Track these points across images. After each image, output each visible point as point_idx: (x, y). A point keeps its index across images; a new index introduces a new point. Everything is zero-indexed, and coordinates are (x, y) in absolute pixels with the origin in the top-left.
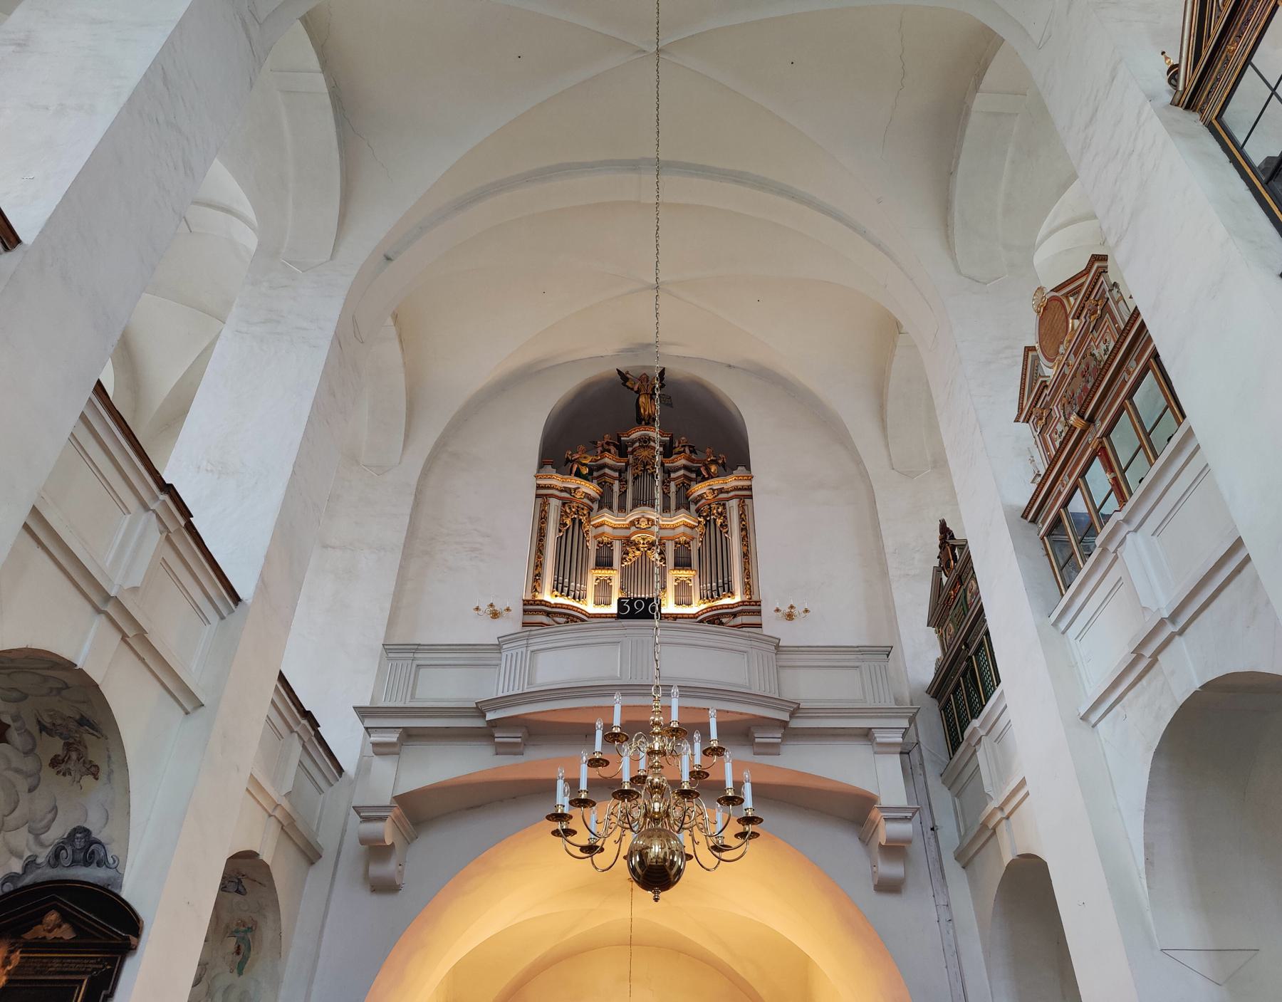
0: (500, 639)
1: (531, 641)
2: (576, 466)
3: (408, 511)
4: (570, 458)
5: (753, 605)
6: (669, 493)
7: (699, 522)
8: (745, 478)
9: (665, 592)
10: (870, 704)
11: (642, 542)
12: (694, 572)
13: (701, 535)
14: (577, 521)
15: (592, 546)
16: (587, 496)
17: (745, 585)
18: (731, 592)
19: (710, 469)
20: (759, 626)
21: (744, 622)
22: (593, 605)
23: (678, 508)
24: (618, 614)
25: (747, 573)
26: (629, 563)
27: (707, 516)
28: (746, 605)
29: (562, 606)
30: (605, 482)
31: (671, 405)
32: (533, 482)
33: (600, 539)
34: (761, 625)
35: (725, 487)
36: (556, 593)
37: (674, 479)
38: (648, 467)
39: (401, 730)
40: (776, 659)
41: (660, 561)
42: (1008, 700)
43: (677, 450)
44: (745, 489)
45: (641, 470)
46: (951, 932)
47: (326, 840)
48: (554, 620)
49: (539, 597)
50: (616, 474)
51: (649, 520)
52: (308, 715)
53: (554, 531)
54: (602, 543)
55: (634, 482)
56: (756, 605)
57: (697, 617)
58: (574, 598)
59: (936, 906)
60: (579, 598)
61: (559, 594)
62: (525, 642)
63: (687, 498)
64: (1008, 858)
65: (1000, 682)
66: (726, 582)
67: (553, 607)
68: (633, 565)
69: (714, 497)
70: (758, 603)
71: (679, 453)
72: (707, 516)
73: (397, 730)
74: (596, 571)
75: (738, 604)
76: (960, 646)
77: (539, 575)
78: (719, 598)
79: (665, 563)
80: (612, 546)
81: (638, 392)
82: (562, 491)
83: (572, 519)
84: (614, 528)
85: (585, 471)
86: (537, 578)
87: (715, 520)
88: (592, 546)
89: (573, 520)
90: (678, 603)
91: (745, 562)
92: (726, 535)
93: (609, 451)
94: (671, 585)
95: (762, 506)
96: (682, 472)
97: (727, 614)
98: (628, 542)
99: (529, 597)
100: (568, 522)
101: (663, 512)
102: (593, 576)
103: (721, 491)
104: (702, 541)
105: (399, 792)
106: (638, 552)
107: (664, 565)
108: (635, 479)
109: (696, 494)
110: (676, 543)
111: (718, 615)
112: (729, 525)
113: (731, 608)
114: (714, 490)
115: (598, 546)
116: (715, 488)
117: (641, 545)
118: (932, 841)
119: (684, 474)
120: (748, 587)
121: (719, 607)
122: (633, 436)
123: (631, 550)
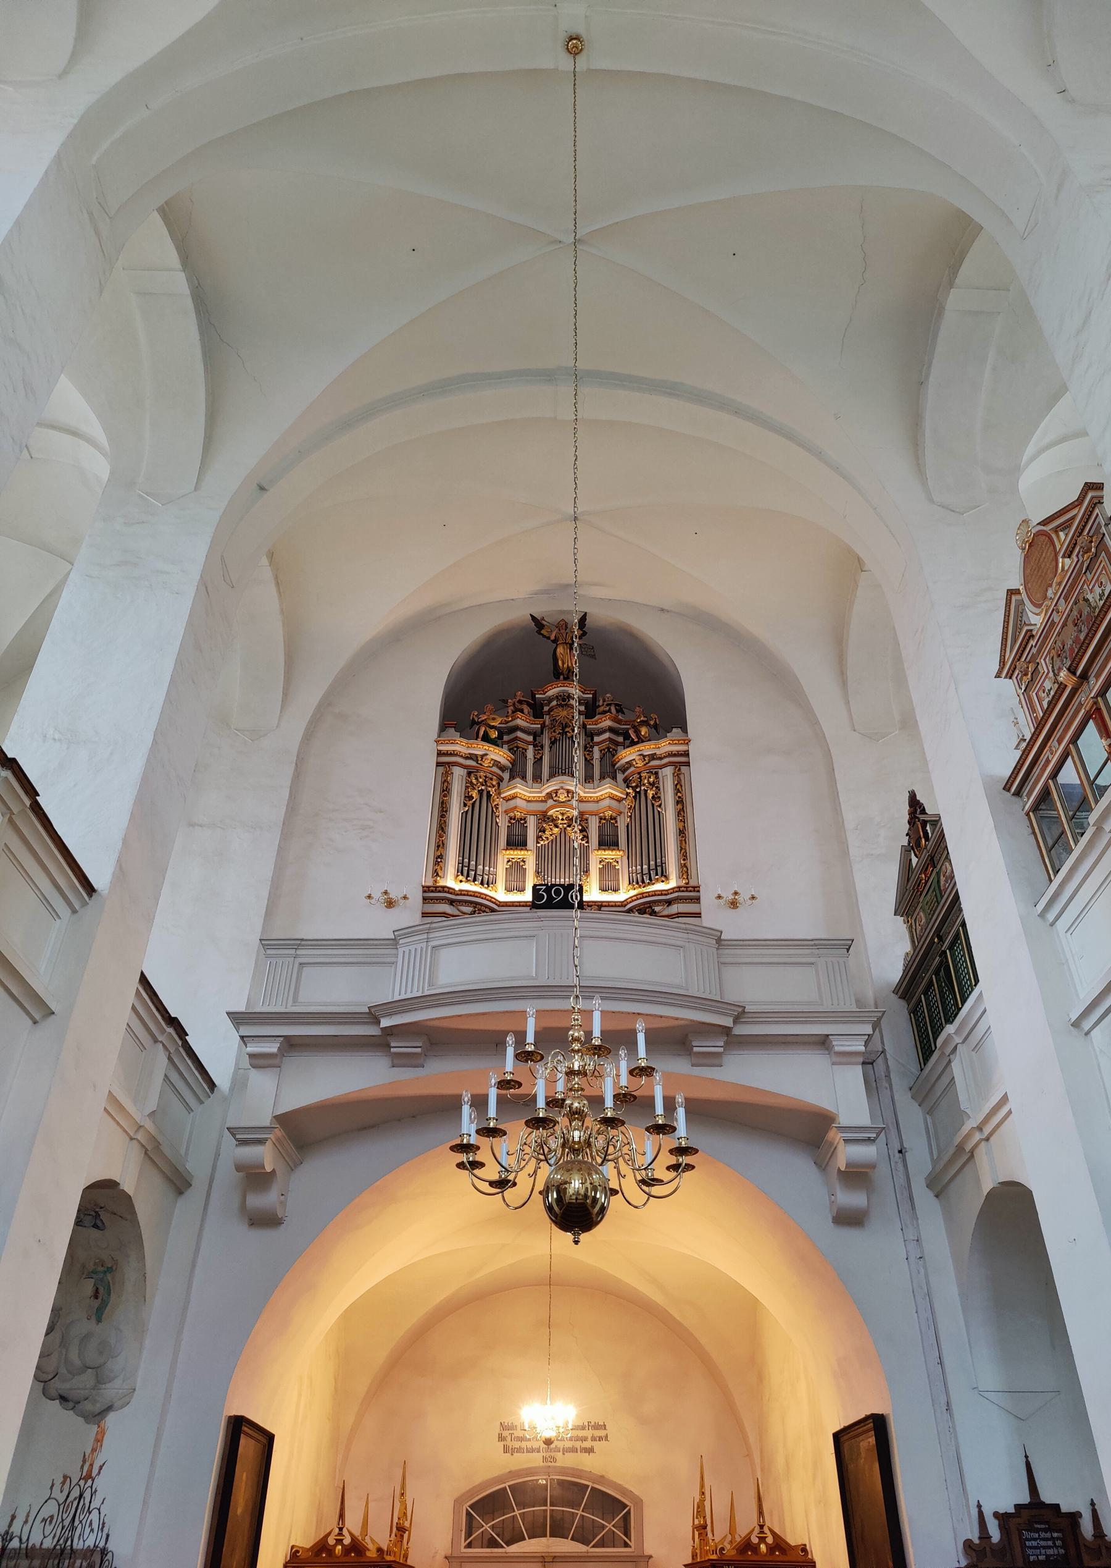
0: (396, 933)
1: (431, 935)
2: (482, 730)
3: (289, 783)
4: (476, 719)
5: (691, 891)
7: (628, 794)
8: (680, 742)
9: (587, 877)
10: (827, 1006)
11: (560, 817)
12: (621, 853)
13: (630, 809)
15: (503, 822)
16: (496, 763)
17: (682, 867)
18: (665, 876)
19: (640, 732)
20: (698, 915)
23: (602, 778)
24: (533, 902)
25: (683, 854)
26: (546, 842)
27: (637, 786)
28: (683, 891)
29: (467, 893)
30: (518, 747)
31: (593, 657)
33: (512, 814)
34: (700, 914)
35: (658, 752)
36: (461, 878)
37: (598, 744)
38: (567, 730)
39: (282, 1039)
40: (717, 953)
41: (582, 840)
42: (988, 1002)
43: (601, 709)
44: (681, 755)
45: (559, 733)
46: (922, 1271)
47: (196, 1166)
48: (458, 909)
49: (441, 883)
50: (530, 738)
51: (568, 791)
52: (174, 1022)
53: (458, 805)
54: (514, 819)
55: (551, 748)
56: (694, 891)
57: (626, 905)
58: (482, 883)
59: (904, 1241)
60: (488, 884)
61: (464, 879)
62: (425, 936)
63: (614, 766)
64: (987, 1186)
65: (978, 981)
66: (659, 863)
67: (458, 895)
68: (550, 844)
69: (645, 765)
70: (696, 889)
71: (604, 712)
72: (637, 786)
73: (277, 1039)
74: (508, 852)
75: (673, 890)
76: (932, 939)
77: (441, 856)
78: (651, 882)
80: (526, 822)
81: (555, 641)
82: (467, 758)
83: (479, 791)
85: (494, 734)
87: (646, 791)
88: (503, 822)
89: (481, 792)
90: (603, 889)
92: (659, 809)
93: (522, 711)
95: (699, 775)
96: (607, 735)
98: (544, 818)
99: (430, 883)
100: (475, 794)
101: (586, 782)
102: (504, 858)
103: (653, 757)
104: (631, 816)
105: (280, 1111)
106: (557, 829)
107: (586, 845)
108: (553, 743)
109: (623, 761)
110: (601, 819)
112: (662, 798)
113: (665, 895)
114: (644, 756)
115: (509, 822)
117: (560, 822)
118: (900, 1166)
120: (685, 870)
122: (550, 693)
123: (547, 827)
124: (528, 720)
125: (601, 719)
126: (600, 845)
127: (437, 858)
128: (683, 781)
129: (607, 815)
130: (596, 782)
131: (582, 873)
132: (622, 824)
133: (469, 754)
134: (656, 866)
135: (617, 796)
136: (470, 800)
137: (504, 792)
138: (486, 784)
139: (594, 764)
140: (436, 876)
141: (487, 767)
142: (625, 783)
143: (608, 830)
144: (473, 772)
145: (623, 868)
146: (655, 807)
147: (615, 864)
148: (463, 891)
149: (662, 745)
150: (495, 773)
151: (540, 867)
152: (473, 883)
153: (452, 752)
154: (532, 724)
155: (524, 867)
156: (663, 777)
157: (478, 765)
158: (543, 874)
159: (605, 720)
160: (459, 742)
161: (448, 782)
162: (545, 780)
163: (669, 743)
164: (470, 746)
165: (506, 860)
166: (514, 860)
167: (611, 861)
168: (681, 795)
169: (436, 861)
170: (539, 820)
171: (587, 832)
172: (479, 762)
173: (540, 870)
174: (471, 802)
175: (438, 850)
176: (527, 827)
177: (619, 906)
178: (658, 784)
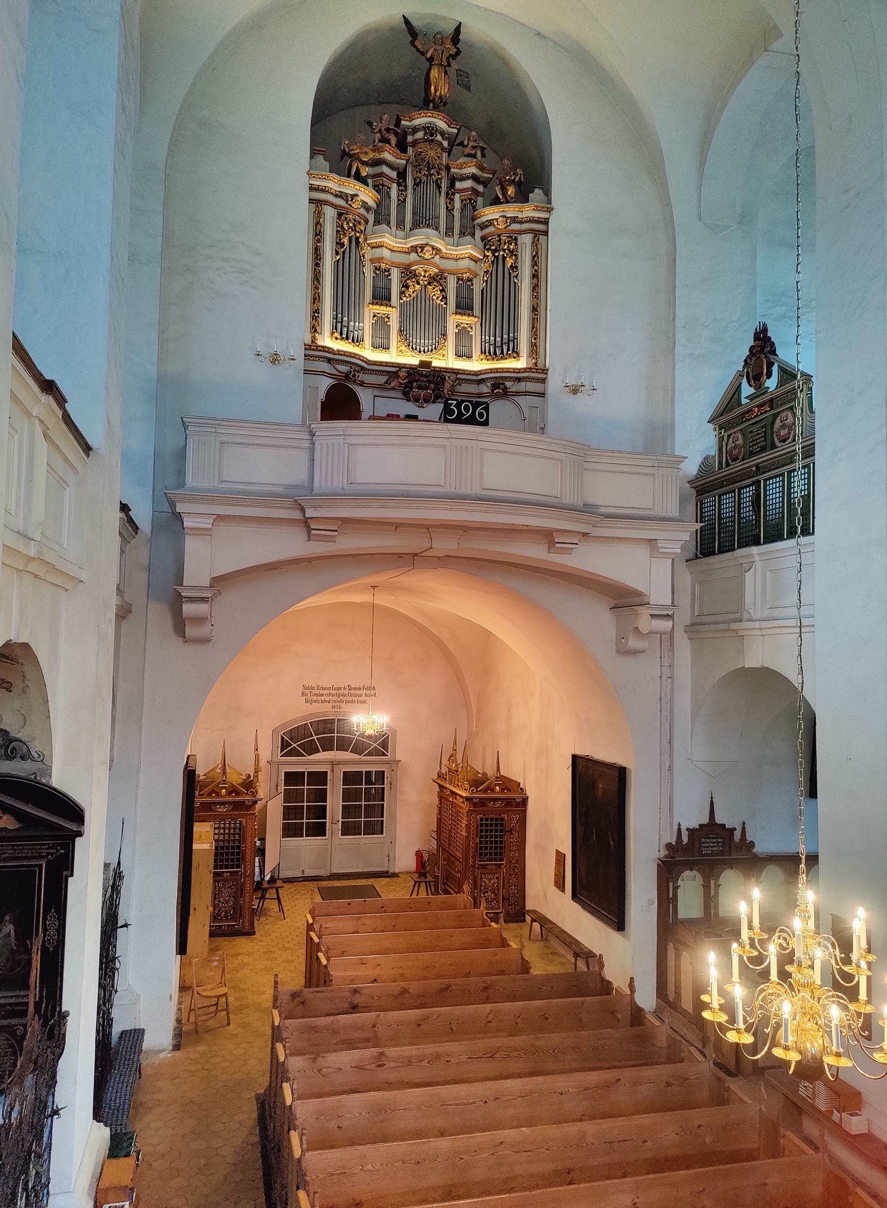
6: (453, 209)
7: (485, 256)
9: (445, 340)
11: (423, 274)
12: (476, 319)
13: (487, 272)
15: (368, 271)
17: (532, 346)
18: (517, 353)
21: (528, 389)
22: (371, 348)
23: (462, 234)
26: (408, 299)
27: (496, 250)
29: (345, 354)
30: (383, 185)
32: (305, 181)
37: (460, 191)
41: (441, 300)
43: (468, 150)
44: (541, 222)
45: (424, 175)
46: (669, 687)
51: (433, 248)
53: (330, 256)
54: (379, 270)
55: (414, 189)
56: (543, 373)
57: (479, 375)
61: (339, 337)
63: (473, 220)
66: (511, 339)
67: (335, 354)
69: (506, 227)
70: (545, 371)
72: (496, 250)
74: (375, 307)
75: (525, 370)
79: (446, 304)
80: (390, 275)
81: (431, 60)
83: (349, 237)
84: (393, 251)
85: (365, 171)
86: (316, 314)
87: (504, 258)
88: (368, 271)
89: (350, 239)
90: (459, 355)
91: (533, 319)
92: (515, 280)
93: (388, 141)
94: (451, 331)
96: (469, 184)
97: (511, 378)
101: (446, 236)
102: (370, 311)
103: (514, 220)
104: (487, 281)
106: (419, 286)
107: (444, 306)
108: (417, 184)
109: (484, 219)
110: (458, 279)
111: (501, 377)
112: (519, 268)
113: (517, 373)
114: (507, 218)
115: (374, 272)
116: (508, 216)
117: (421, 278)
120: (534, 349)
121: (504, 370)
122: (416, 122)
123: (411, 284)
124: (394, 154)
125: (467, 164)
126: (457, 308)
128: (540, 252)
129: (464, 276)
131: (440, 336)
132: (478, 286)
133: (340, 192)
134: (509, 340)
135: (475, 257)
136: (341, 248)
138: (355, 230)
139: (455, 215)
140: (314, 332)
141: (356, 209)
142: (482, 241)
143: (464, 293)
145: (476, 333)
146: (512, 278)
147: (470, 329)
149: (526, 209)
150: (362, 215)
151: (402, 325)
152: (347, 341)
153: (324, 188)
154: (398, 158)
155: (388, 323)
157: (348, 206)
158: (405, 332)
159: (470, 166)
160: (332, 179)
161: (321, 225)
163: (533, 209)
164: (342, 183)
166: (379, 315)
167: (466, 326)
168: (537, 268)
169: (314, 316)
170: (402, 273)
171: (445, 293)
173: (402, 328)
176: (391, 279)
177: (473, 375)
178: (517, 251)
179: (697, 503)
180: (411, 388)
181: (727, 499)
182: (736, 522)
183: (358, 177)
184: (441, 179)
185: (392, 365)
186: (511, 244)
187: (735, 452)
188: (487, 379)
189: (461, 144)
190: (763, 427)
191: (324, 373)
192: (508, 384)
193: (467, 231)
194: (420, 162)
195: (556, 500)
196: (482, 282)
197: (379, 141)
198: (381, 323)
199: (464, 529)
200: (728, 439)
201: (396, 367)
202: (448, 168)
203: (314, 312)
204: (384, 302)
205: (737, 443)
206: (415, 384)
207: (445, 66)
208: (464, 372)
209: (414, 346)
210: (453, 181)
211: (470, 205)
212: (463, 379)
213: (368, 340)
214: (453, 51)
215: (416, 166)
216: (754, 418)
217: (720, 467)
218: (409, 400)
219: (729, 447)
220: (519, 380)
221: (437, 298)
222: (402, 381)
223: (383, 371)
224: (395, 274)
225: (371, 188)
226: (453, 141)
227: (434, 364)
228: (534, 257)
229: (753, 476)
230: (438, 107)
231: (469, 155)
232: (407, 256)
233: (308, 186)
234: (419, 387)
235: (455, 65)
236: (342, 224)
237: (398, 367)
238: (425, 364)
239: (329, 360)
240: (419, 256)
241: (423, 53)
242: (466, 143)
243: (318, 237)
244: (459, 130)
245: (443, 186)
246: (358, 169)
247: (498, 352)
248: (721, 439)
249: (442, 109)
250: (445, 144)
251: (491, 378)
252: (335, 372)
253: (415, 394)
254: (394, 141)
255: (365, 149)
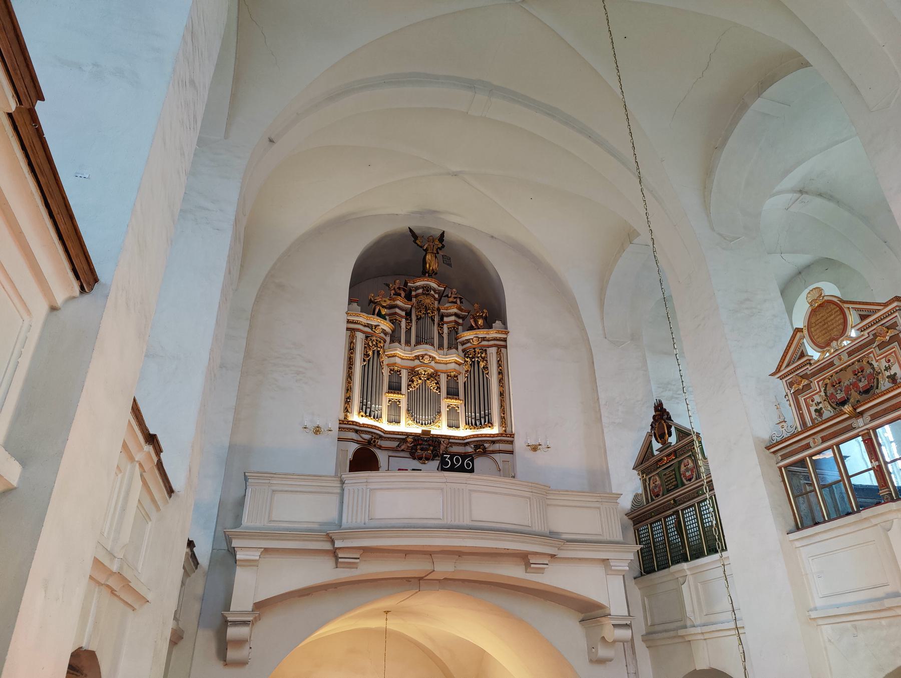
4: (372, 299)
5: (508, 437)
6: (443, 334)
7: (465, 361)
9: (440, 416)
11: (423, 373)
12: (461, 402)
13: (467, 371)
14: (376, 352)
16: (384, 331)
18: (491, 423)
19: (478, 322)
21: (501, 448)
22: (387, 422)
23: (449, 348)
26: (413, 389)
28: (504, 436)
29: (368, 426)
30: (396, 320)
31: (450, 265)
32: (345, 318)
33: (392, 368)
34: (513, 452)
35: (488, 336)
37: (447, 323)
38: (428, 311)
39: (263, 550)
41: (437, 390)
43: (451, 300)
44: (502, 340)
45: (423, 314)
49: (350, 419)
50: (403, 314)
51: (430, 357)
54: (393, 371)
56: (511, 437)
59: (628, 673)
61: (364, 415)
63: (456, 339)
67: (361, 427)
68: (416, 391)
69: (478, 344)
70: (512, 435)
73: (259, 549)
74: (390, 395)
75: (498, 435)
77: (349, 398)
79: (440, 392)
80: (400, 374)
81: (426, 250)
82: (365, 326)
83: (373, 351)
85: (384, 311)
86: (348, 400)
87: (478, 363)
88: (386, 372)
90: (450, 426)
93: (400, 295)
96: (453, 318)
99: (342, 418)
100: (370, 353)
103: (484, 339)
106: (420, 381)
107: (439, 393)
108: (418, 319)
109: (464, 339)
110: (448, 376)
111: (481, 441)
112: (489, 368)
113: (492, 437)
114: (479, 338)
117: (422, 375)
119: (455, 320)
120: (503, 421)
121: (483, 436)
122: (418, 284)
126: (448, 394)
127: (347, 399)
128: (502, 358)
130: (445, 350)
132: (461, 380)
133: (367, 324)
137: (387, 352)
138: (377, 346)
142: (463, 352)
143: (452, 385)
144: (369, 336)
145: (461, 411)
146: (484, 374)
147: (457, 408)
148: (365, 424)
152: (370, 418)
156: (490, 353)
157: (373, 332)
162: (413, 345)
165: (388, 400)
169: (346, 401)
172: (373, 330)
174: (368, 358)
175: (347, 392)
176: (401, 377)
177: (460, 439)
179: (635, 531)
180: (416, 450)
181: (657, 526)
182: (667, 545)
183: (379, 315)
184: (434, 316)
185: (402, 433)
186: (483, 354)
187: (656, 490)
188: (471, 442)
189: (447, 296)
190: (672, 471)
191: (352, 440)
192: (486, 445)
193: (453, 345)
194: (420, 306)
195: (529, 529)
196: (464, 377)
197: (394, 295)
198: (394, 406)
199: (458, 554)
200: (649, 481)
201: (405, 435)
202: (439, 310)
203: (347, 399)
204: (396, 392)
205: (657, 483)
206: (419, 447)
207: (435, 254)
208: (454, 438)
209: (418, 421)
210: (442, 317)
211: (454, 332)
212: (453, 443)
213: (385, 418)
214: (440, 245)
215: (418, 309)
216: (665, 464)
217: (648, 502)
218: (414, 459)
219: (651, 486)
220: (494, 442)
221: (434, 388)
222: (409, 445)
223: (395, 438)
224: (404, 375)
225: (388, 321)
226: (441, 295)
227: (432, 433)
228: (498, 361)
229: (673, 508)
230: (431, 276)
231: (452, 302)
232: (412, 362)
233: (346, 320)
234: (422, 449)
235: (441, 253)
236: (368, 343)
237: (407, 435)
238: (426, 433)
239: (356, 431)
240: (421, 362)
241: (421, 247)
242: (450, 295)
243: (352, 351)
244: (445, 288)
245: (436, 320)
246: (379, 310)
247: (478, 423)
248: (644, 481)
249: (433, 276)
250: (437, 296)
251: (474, 441)
252: (360, 439)
253: (419, 454)
254: (403, 294)
255: (384, 299)
